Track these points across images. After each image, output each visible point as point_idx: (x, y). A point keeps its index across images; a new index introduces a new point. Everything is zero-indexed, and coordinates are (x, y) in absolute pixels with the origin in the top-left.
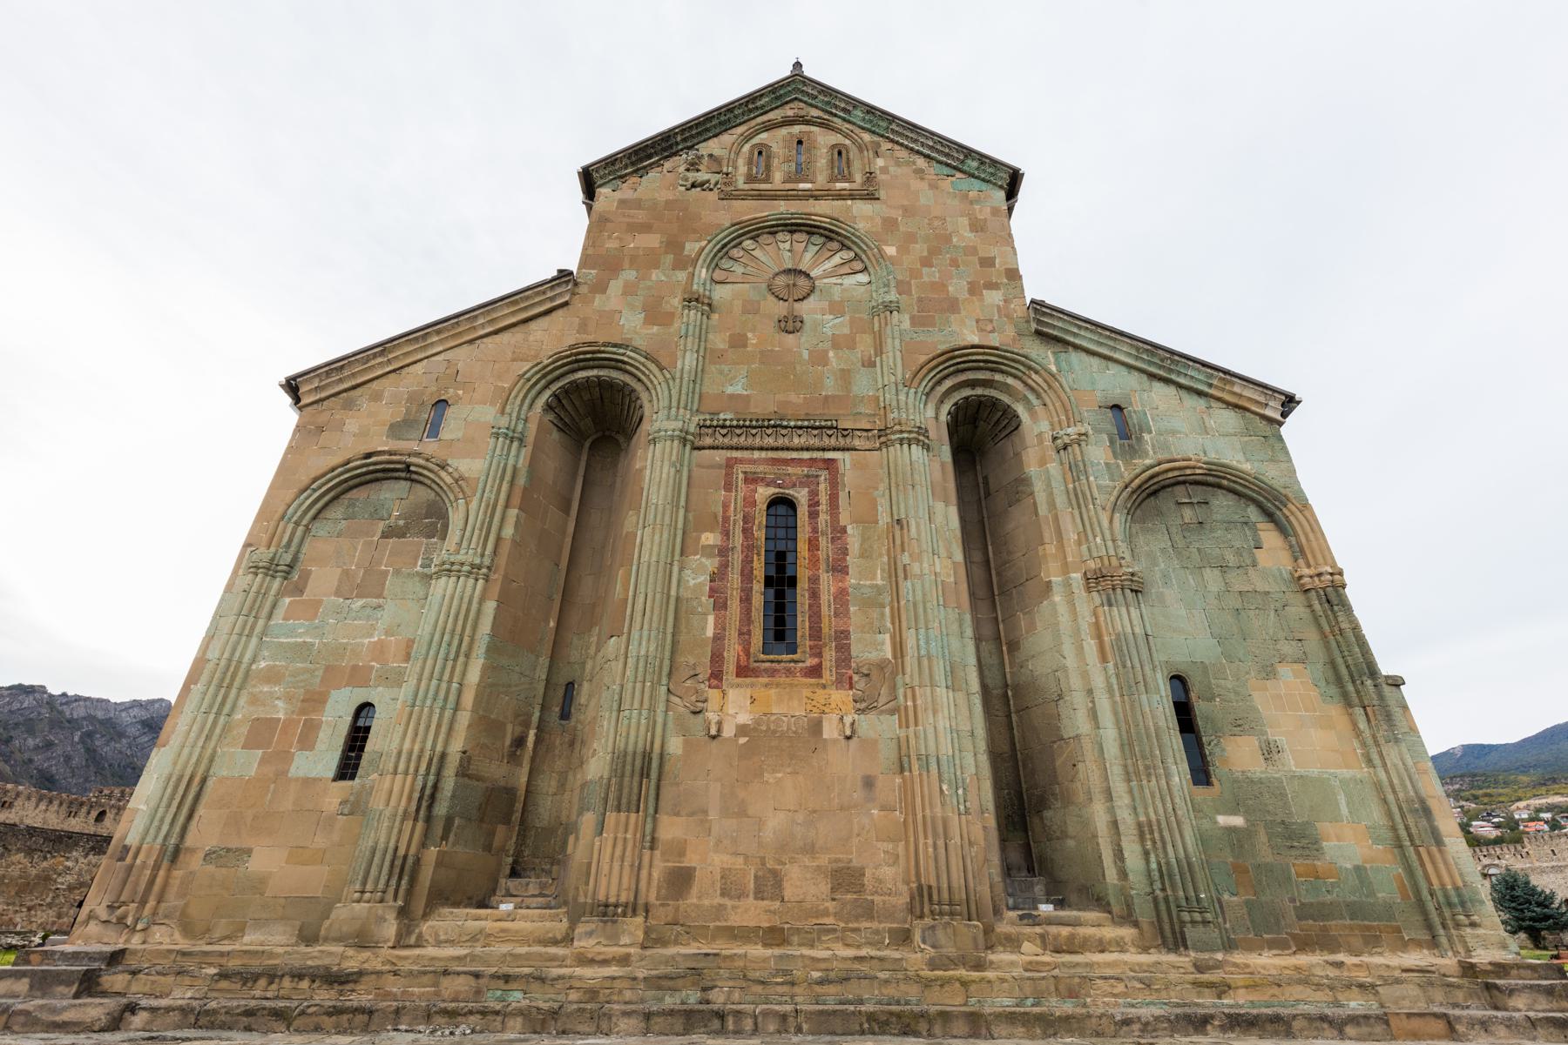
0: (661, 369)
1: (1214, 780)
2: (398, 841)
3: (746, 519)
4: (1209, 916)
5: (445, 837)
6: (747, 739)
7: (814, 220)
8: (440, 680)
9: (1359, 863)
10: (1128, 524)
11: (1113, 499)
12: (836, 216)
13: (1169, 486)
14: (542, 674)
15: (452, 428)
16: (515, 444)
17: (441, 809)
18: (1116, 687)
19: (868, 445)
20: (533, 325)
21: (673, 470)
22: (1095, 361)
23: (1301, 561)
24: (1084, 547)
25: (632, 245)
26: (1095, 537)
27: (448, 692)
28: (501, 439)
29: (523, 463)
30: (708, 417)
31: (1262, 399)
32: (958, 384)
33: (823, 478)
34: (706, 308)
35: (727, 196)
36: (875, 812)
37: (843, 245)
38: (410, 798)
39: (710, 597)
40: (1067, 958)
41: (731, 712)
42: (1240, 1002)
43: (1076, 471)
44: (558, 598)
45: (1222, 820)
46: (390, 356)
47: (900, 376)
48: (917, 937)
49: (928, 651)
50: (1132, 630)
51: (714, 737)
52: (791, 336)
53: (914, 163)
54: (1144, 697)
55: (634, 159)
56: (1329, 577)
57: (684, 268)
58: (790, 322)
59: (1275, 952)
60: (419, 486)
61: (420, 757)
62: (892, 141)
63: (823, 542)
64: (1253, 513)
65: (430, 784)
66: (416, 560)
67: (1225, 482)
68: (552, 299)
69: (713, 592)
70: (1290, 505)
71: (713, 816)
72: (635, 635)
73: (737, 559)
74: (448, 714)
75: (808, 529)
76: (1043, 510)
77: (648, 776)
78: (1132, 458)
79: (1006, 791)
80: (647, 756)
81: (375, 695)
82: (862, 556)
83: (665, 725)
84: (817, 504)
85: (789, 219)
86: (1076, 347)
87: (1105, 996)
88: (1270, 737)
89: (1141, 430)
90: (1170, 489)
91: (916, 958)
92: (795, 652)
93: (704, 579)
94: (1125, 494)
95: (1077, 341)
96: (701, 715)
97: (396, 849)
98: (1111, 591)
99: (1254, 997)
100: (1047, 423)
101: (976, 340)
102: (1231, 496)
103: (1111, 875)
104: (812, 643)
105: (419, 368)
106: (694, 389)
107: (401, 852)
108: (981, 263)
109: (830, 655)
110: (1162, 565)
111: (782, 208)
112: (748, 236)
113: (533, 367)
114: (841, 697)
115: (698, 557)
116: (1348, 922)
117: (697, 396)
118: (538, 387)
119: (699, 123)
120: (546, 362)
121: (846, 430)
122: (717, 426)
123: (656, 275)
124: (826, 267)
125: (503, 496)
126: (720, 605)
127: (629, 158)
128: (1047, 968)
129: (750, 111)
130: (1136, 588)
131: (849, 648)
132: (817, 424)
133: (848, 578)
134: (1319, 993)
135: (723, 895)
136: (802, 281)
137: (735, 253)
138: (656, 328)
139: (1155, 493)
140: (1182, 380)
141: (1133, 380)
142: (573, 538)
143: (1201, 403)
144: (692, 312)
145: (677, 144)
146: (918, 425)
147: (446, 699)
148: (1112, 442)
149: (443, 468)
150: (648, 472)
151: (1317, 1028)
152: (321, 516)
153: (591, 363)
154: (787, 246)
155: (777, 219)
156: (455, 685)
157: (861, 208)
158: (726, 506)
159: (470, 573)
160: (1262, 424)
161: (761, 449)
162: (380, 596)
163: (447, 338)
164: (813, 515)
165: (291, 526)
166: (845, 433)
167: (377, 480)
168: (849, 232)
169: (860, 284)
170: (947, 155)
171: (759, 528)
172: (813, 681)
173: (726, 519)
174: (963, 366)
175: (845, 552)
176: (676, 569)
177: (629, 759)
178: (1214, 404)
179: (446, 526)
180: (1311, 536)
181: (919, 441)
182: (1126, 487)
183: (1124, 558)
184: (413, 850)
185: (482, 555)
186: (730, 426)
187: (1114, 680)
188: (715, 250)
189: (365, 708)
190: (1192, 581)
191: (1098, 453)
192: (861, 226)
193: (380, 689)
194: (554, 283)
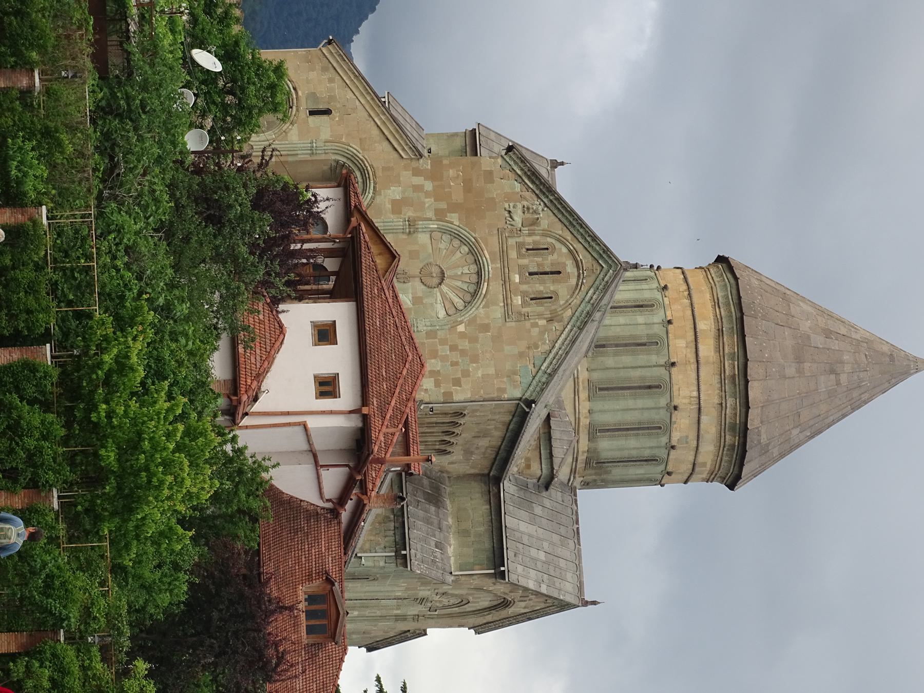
16: (309, 152)
20: (386, 143)
25: (452, 184)
34: (407, 230)
35: (500, 232)
46: (355, 81)
53: (544, 343)
55: (529, 174)
57: (436, 215)
58: (403, 276)
108: (456, 379)
111: (491, 267)
112: (471, 249)
123: (429, 201)
136: (436, 281)
138: (390, 206)
144: (402, 223)
153: (364, 178)
157: (497, 312)
188: (453, 230)
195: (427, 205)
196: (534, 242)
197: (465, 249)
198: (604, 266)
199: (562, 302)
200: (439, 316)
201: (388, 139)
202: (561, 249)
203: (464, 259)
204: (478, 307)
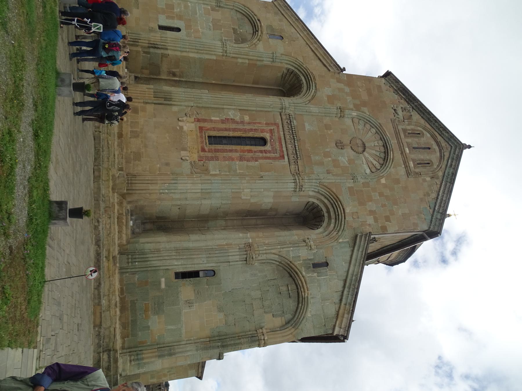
0: (310, 101)
1: (177, 280)
2: (142, 39)
3: (255, 130)
4: (130, 264)
5: (145, 52)
6: (179, 129)
7: (390, 153)
8: (189, 45)
9: (151, 328)
10: (274, 262)
11: (284, 255)
12: (395, 161)
13: (295, 282)
14: (197, 80)
15: (273, 42)
17: (152, 50)
18: (208, 248)
19: (293, 170)
20: (318, 61)
21: (269, 105)
22: (348, 258)
23: (269, 331)
24: (263, 244)
25: (360, 90)
26: (267, 247)
27: (186, 48)
28: (272, 55)
29: (265, 63)
30: (293, 117)
31: (343, 326)
32: (327, 206)
33: (276, 155)
34: (339, 115)
35: (393, 121)
36: (158, 166)
37: (382, 165)
38: (154, 41)
39: (226, 118)
40: (116, 220)
41: (187, 124)
42: (104, 263)
43: (295, 244)
44: (223, 83)
45: (163, 280)
46: (296, 22)
47: (323, 181)
48: (121, 172)
49: (214, 183)
50: (230, 256)
51: (178, 119)
52: (335, 145)
53: (432, 193)
54: (204, 256)
56: (262, 338)
58: (340, 145)
59: (119, 289)
60: (252, 35)
61: (166, 42)
62: (441, 184)
63: (252, 154)
64: (289, 316)
65: (158, 46)
66: (227, 37)
67: (300, 305)
68: (330, 66)
69: (228, 119)
70: (293, 330)
71: (154, 119)
72: (209, 95)
73: (240, 127)
74: (180, 49)
75: (255, 150)
76: (277, 233)
77: (165, 100)
78: (304, 267)
79: (170, 226)
80: (170, 99)
81: (183, 32)
82: (247, 166)
83: (181, 105)
84: (266, 153)
85: (389, 144)
86: (353, 251)
87: (105, 221)
88: (195, 304)
89: (318, 273)
90: (294, 283)
91: (114, 171)
92: (209, 144)
93: (232, 117)
94: (287, 261)
95: (355, 251)
96: (185, 116)
97: (140, 39)
98: (245, 250)
99: (106, 269)
100: (316, 237)
101: (347, 210)
102: (295, 308)
103: (142, 240)
104: (213, 149)
105: (293, 30)
106: (304, 112)
107: (139, 41)
109: (210, 155)
110: (259, 275)
111: (393, 142)
113: (301, 62)
114: (195, 157)
115: (239, 115)
116: (130, 319)
117: (301, 113)
118: (294, 65)
119: (425, 110)
120: (304, 66)
121: (297, 163)
122: (290, 120)
123: (349, 99)
124: (370, 158)
125: (252, 58)
126: (223, 122)
127: (401, 87)
128: (113, 209)
129: (439, 129)
130: (247, 260)
131: (213, 160)
132: (298, 153)
133: (238, 161)
134: (107, 291)
135: (131, 122)
136: (361, 149)
137: (368, 126)
138: (326, 99)
139: (291, 276)
140: (345, 292)
141: (342, 272)
142: (245, 86)
143: (337, 300)
145: (413, 104)
146: (303, 186)
147: (184, 48)
148: (310, 260)
149: (258, 40)
150: (268, 98)
151: (97, 281)
152: (238, 12)
153: (307, 80)
154: (376, 144)
155: (387, 140)
156: (188, 50)
157: (402, 171)
158: (260, 123)
159: (224, 50)
160: (331, 325)
161: (284, 134)
162: (214, 29)
163: (307, 37)
164: (261, 152)
165: (232, 4)
166: (296, 163)
167: (252, 24)
168: (388, 165)
169: (365, 171)
170: (440, 206)
171: (252, 133)
172: (200, 149)
173: (255, 123)
174: (335, 206)
175: (248, 161)
176: (234, 107)
177: (170, 94)
178: (337, 306)
179: (239, 43)
180: (280, 335)
181: (297, 186)
182: (290, 262)
183: (259, 256)
184: (140, 44)
185: (230, 53)
186: (291, 124)
187: (210, 247)
188: (366, 118)
189: (178, 30)
190: (254, 285)
191: (304, 253)
192: (392, 170)
193: (185, 33)
194: (336, 65)
195: (348, 101)
196: (412, 130)
197: (373, 130)
198: (452, 146)
199: (435, 167)
200: (367, 173)
201: (319, 59)
202: (426, 134)
203: (374, 137)
204: (390, 167)
